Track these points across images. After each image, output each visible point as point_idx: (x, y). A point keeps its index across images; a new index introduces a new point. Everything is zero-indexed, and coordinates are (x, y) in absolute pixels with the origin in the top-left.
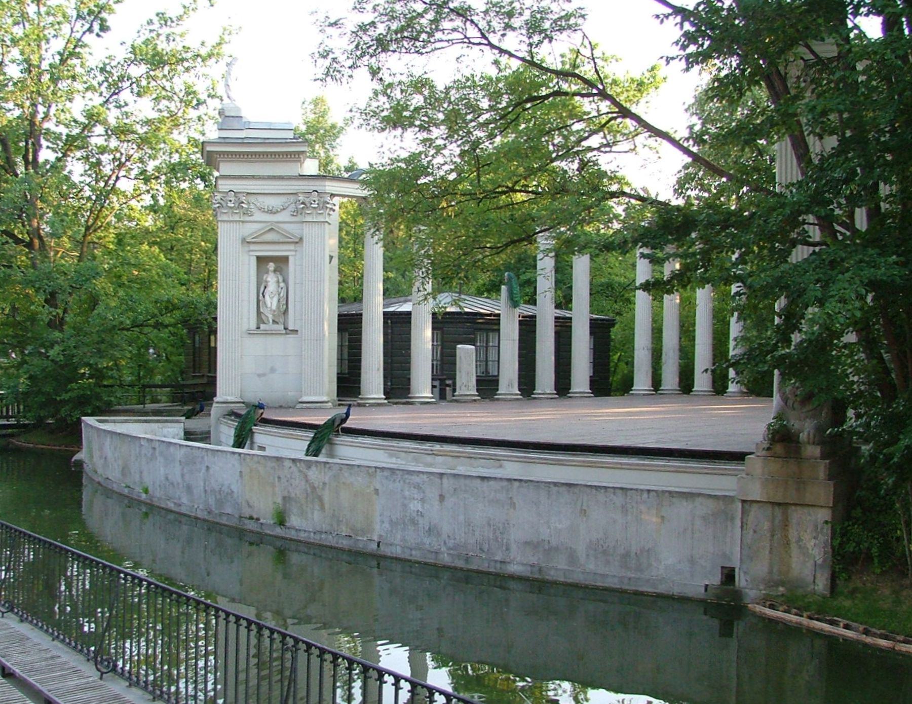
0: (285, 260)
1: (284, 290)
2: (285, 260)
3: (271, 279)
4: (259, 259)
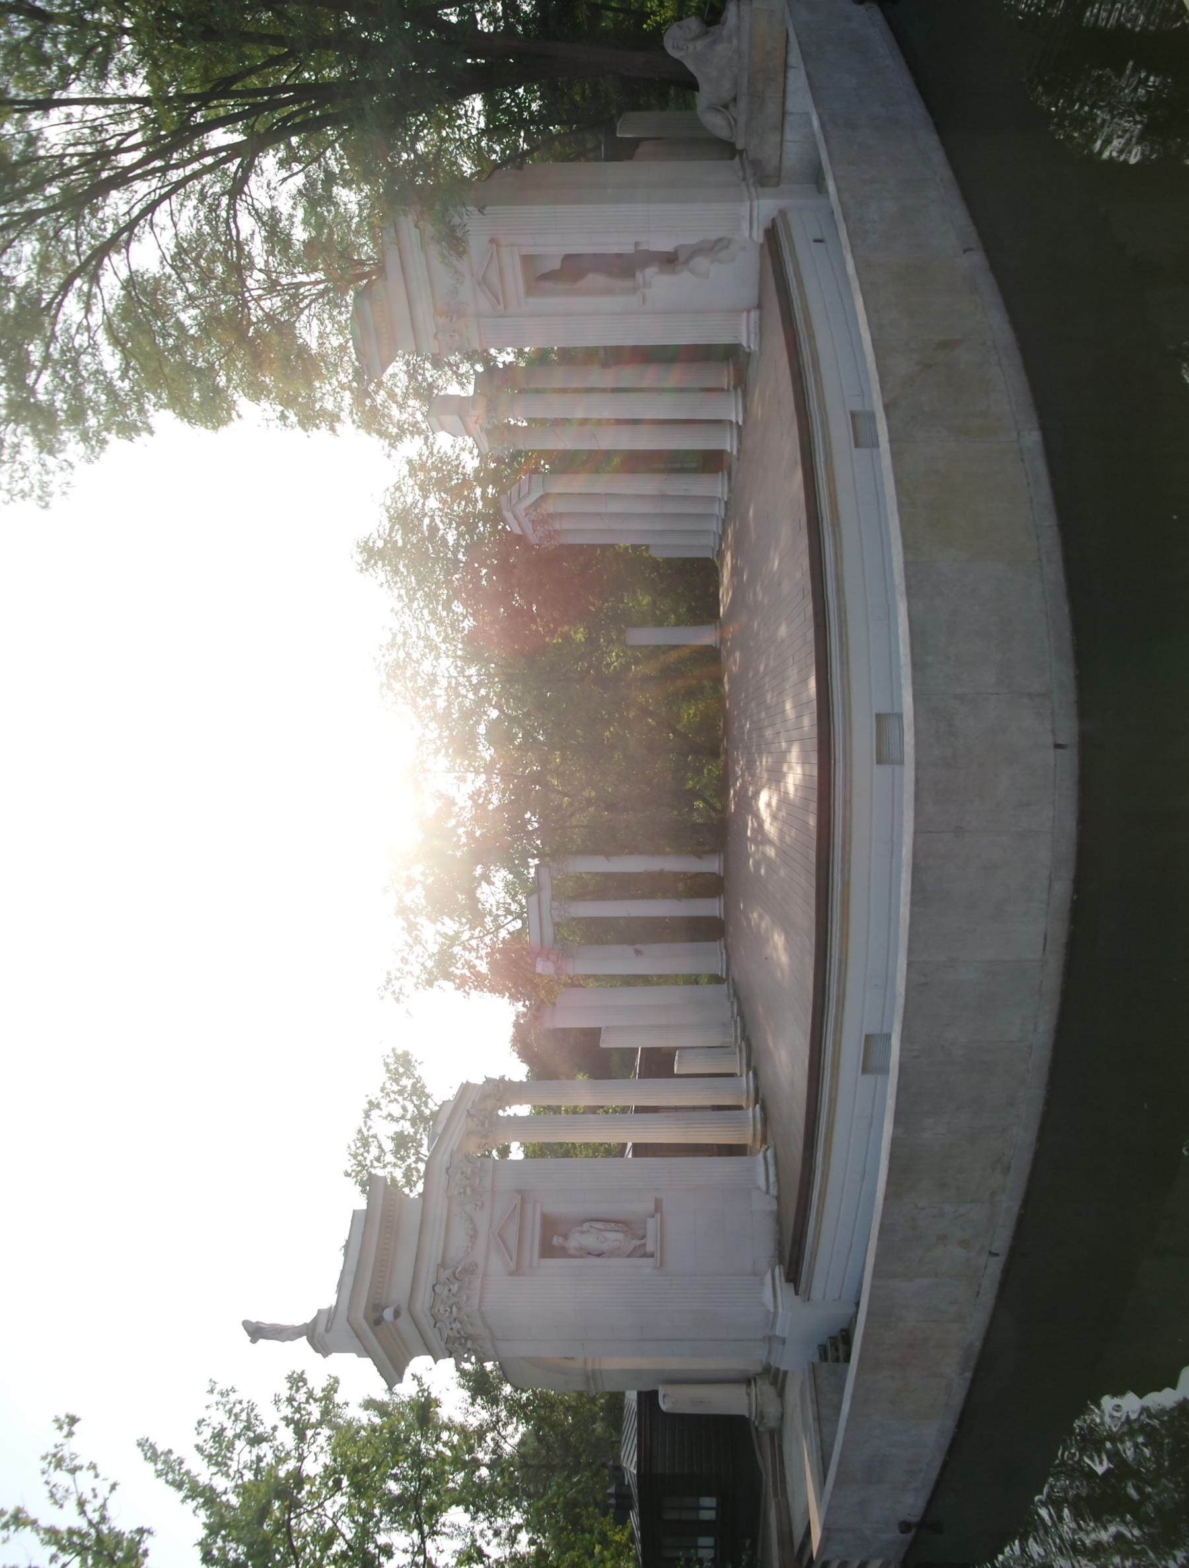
3: (576, 1240)
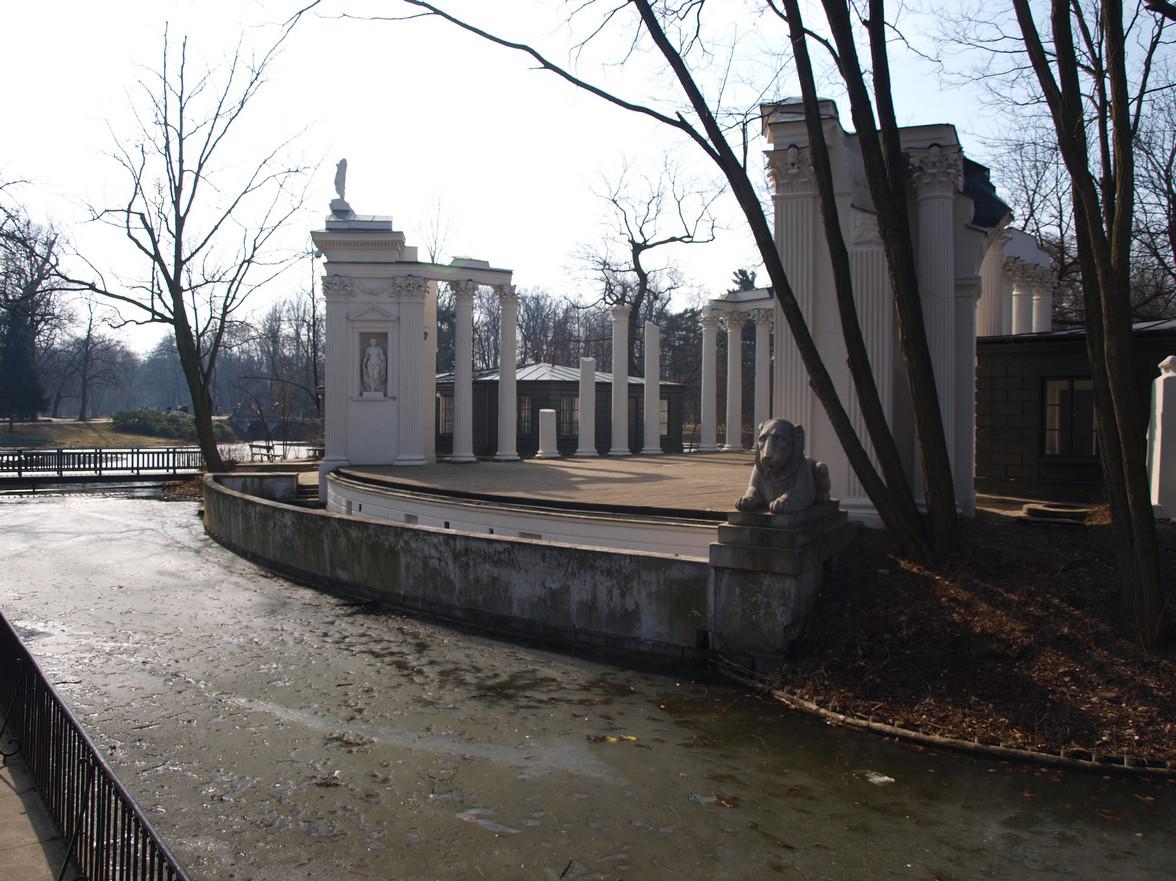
0: (384, 336)
1: (384, 362)
2: (384, 336)
3: (374, 352)
4: (362, 335)
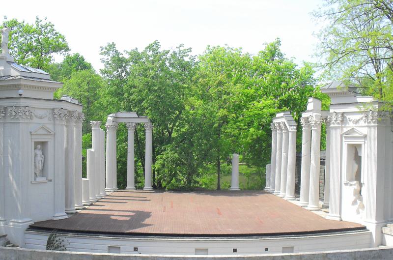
2: (46, 142)
3: (39, 153)
